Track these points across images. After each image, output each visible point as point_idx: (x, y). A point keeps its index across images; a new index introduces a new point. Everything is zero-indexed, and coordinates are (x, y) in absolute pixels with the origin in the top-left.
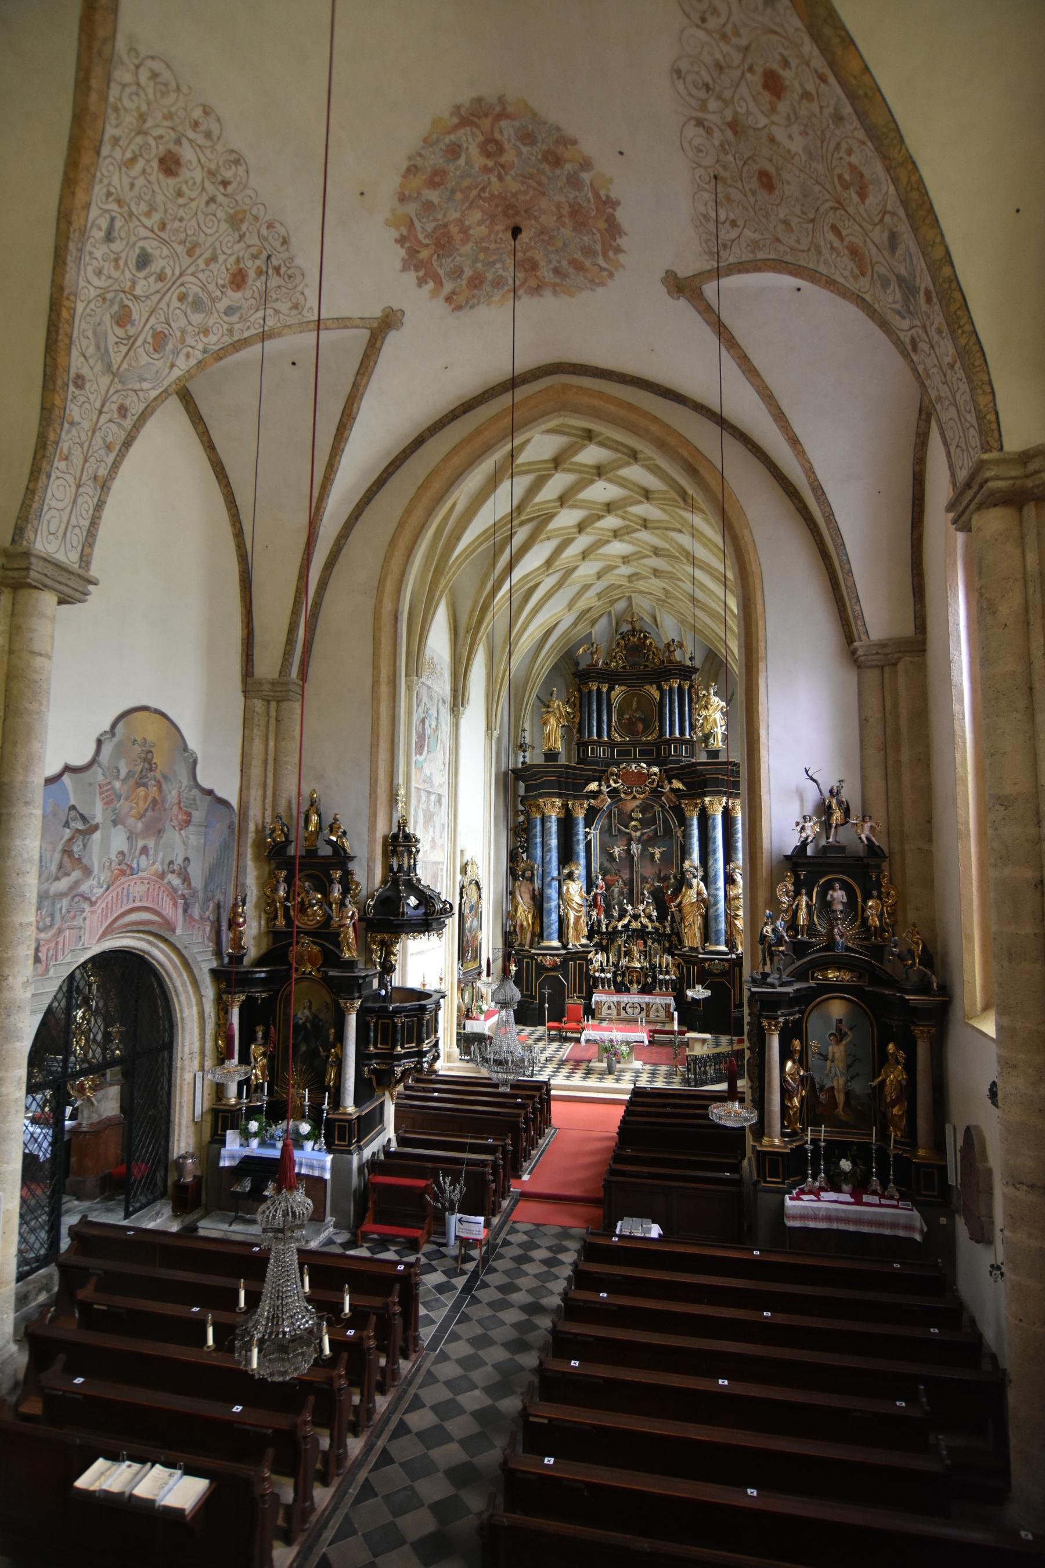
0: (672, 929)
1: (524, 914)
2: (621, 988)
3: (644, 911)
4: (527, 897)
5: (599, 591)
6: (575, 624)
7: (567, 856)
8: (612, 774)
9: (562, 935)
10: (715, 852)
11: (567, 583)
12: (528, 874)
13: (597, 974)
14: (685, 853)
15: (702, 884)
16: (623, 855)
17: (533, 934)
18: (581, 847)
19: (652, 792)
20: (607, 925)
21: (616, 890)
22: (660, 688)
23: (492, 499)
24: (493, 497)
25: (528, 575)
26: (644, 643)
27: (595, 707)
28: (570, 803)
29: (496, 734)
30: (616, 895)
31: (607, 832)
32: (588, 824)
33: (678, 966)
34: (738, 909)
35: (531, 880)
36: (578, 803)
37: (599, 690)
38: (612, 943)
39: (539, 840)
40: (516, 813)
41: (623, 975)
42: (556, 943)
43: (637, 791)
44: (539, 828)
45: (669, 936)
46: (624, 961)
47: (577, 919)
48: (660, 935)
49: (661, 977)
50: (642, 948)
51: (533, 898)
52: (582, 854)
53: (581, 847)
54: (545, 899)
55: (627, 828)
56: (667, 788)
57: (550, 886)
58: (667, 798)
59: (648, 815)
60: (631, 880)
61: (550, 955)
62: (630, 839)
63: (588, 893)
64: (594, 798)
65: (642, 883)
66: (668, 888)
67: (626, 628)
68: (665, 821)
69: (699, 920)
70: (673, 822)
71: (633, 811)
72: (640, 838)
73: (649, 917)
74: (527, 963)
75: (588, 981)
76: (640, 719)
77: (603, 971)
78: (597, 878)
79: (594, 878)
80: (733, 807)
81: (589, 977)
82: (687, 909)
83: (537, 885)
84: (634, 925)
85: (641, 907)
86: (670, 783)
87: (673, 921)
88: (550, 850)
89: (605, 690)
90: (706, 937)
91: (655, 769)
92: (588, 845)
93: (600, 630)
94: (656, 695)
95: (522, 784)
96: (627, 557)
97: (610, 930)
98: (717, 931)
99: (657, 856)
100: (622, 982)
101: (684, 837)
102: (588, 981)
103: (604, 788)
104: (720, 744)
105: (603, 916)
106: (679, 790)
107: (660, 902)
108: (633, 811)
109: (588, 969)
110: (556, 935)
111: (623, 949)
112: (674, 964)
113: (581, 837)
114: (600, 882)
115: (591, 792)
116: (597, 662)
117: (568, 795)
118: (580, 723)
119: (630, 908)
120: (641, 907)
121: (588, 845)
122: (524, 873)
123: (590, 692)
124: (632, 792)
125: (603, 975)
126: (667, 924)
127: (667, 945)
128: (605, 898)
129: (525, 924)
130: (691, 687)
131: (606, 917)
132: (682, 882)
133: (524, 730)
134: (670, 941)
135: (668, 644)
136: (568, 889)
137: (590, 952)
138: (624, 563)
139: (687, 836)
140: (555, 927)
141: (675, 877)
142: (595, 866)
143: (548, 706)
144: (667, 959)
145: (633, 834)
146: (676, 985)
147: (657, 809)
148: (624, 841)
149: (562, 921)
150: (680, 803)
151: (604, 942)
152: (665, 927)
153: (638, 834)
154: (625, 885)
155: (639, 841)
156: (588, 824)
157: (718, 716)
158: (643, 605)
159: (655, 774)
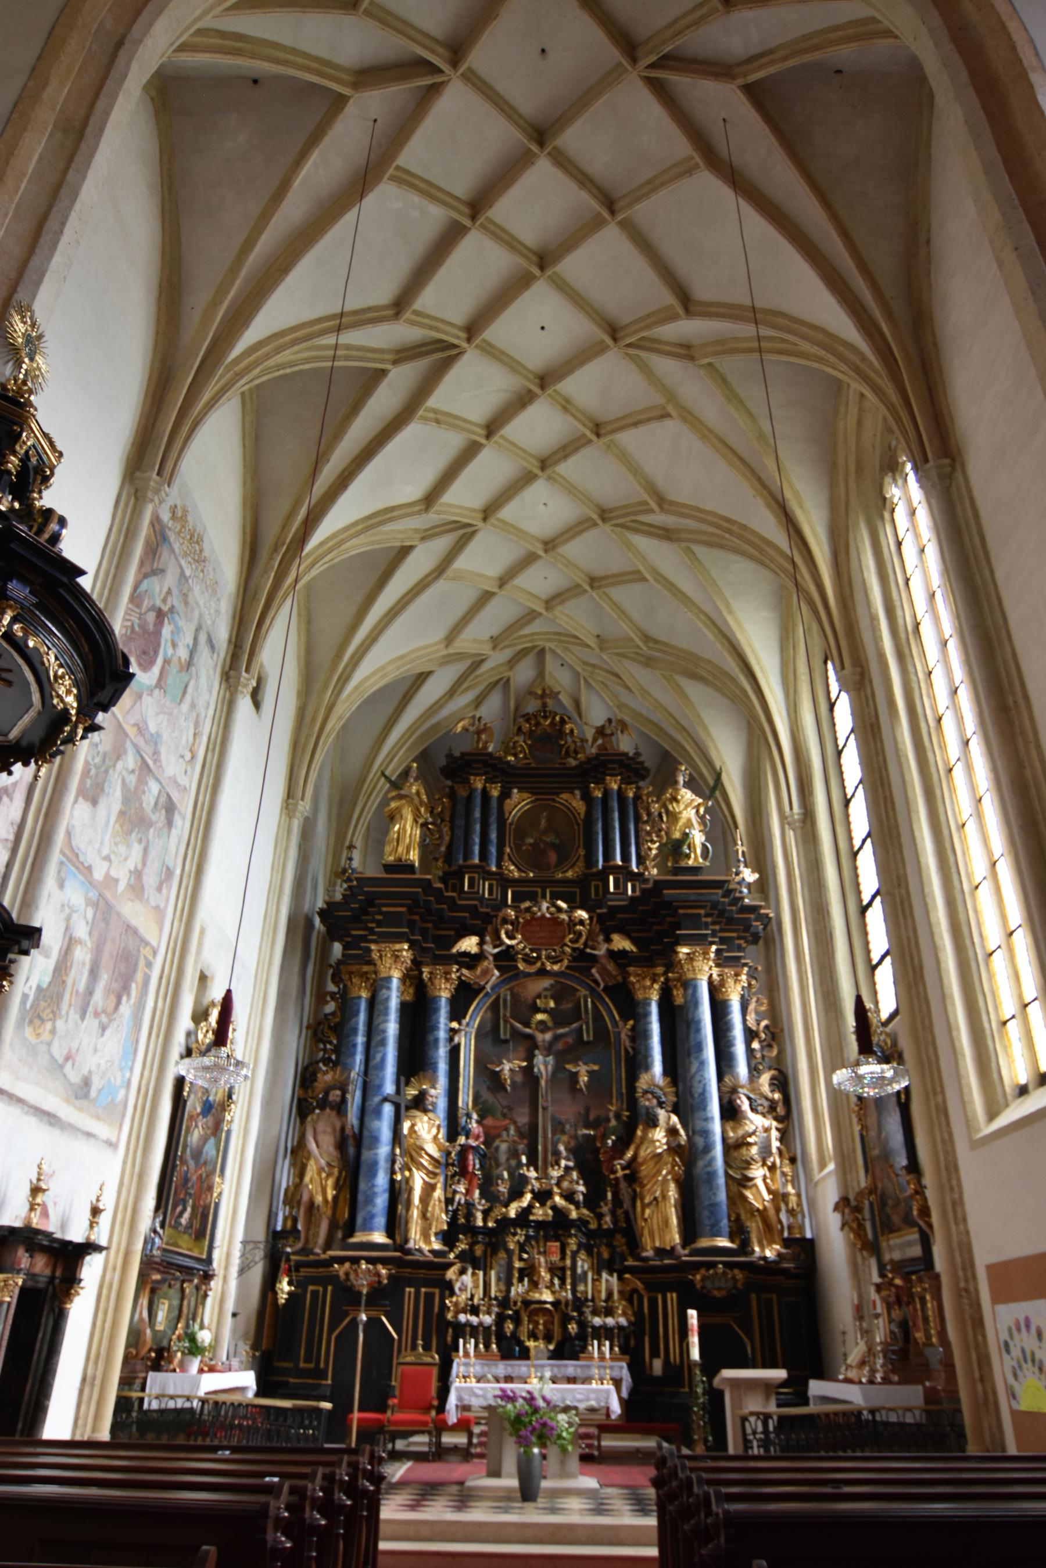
0: (615, 1221)
1: (321, 1185)
2: (511, 1349)
3: (558, 1185)
4: (328, 1141)
5: (494, 631)
6: (451, 693)
7: (414, 1061)
8: (505, 921)
9: (394, 1224)
10: (699, 1047)
11: (449, 573)
12: (335, 1095)
13: (462, 1318)
14: (637, 1063)
15: (674, 1119)
16: (519, 1079)
17: (333, 1226)
18: (442, 1052)
19: (575, 959)
20: (486, 1213)
21: (504, 1147)
22: (587, 797)
23: (350, 217)
24: (357, 208)
25: (392, 509)
26: (561, 733)
27: (477, 814)
28: (426, 970)
29: (304, 807)
30: (503, 1158)
31: (490, 1037)
32: (457, 1013)
33: (629, 1296)
34: (748, 1164)
35: (340, 1108)
36: (440, 969)
37: (485, 792)
38: (495, 1252)
39: (360, 1039)
40: (320, 997)
41: (517, 1320)
42: (379, 1237)
43: (548, 957)
44: (362, 1017)
45: (610, 1234)
46: (518, 1290)
47: (429, 1189)
48: (590, 1234)
49: (597, 1321)
50: (555, 1258)
51: (341, 1145)
52: (443, 1067)
53: (442, 1052)
54: (366, 1142)
55: (527, 1025)
56: (601, 951)
57: (378, 1113)
58: (604, 972)
59: (567, 1006)
60: (533, 1127)
61: (370, 1261)
62: (530, 1047)
63: (452, 1137)
64: (471, 967)
65: (553, 1134)
66: (605, 1137)
67: (532, 706)
68: (598, 1016)
69: (673, 1193)
70: (611, 1013)
71: (539, 996)
72: (551, 1044)
73: (569, 1197)
74: (315, 1294)
75: (442, 1335)
76: (552, 845)
77: (475, 1311)
78: (469, 1116)
79: (463, 1121)
80: (722, 983)
81: (443, 1324)
82: (644, 1170)
83: (352, 1116)
84: (540, 1213)
85: (555, 1173)
86: (608, 940)
87: (617, 1202)
88: (383, 1043)
89: (495, 793)
90: (690, 1229)
91: (583, 914)
92: (454, 1053)
93: (491, 710)
94: (579, 805)
95: (337, 948)
96: (553, 540)
97: (490, 1224)
98: (714, 1206)
99: (584, 1079)
100: (515, 1338)
101: (633, 1039)
102: (442, 1335)
103: (489, 948)
104: (701, 860)
105: (477, 1193)
106: (623, 953)
107: (590, 1163)
108: (539, 996)
109: (444, 1308)
110: (381, 1220)
111: (517, 1264)
112: (620, 1292)
113: (442, 1034)
114: (474, 1126)
115: (466, 954)
116: (485, 747)
117: (424, 951)
118: (450, 847)
119: (532, 1174)
120: (555, 1173)
121: (454, 1053)
122: (327, 1093)
123: (472, 791)
124: (539, 958)
125: (474, 1320)
126: (605, 1209)
127: (606, 1255)
128: (483, 1157)
129: (319, 1199)
130: (637, 797)
131: (482, 1195)
132: (637, 1120)
133: (351, 847)
134: (610, 1246)
135: (603, 727)
136: (413, 1126)
137: (450, 1265)
138: (546, 551)
139: (640, 1035)
140: (381, 1201)
141: (618, 1116)
142: (465, 1098)
143: (401, 789)
144: (609, 1281)
145: (539, 1037)
146: (627, 1339)
147: (583, 992)
148: (522, 1051)
149: (397, 1193)
150: (625, 979)
151: (479, 1251)
152: (600, 1217)
153: (548, 1036)
154: (521, 1135)
155: (549, 1050)
156: (457, 1013)
157: (691, 813)
158: (559, 678)
159: (582, 922)
